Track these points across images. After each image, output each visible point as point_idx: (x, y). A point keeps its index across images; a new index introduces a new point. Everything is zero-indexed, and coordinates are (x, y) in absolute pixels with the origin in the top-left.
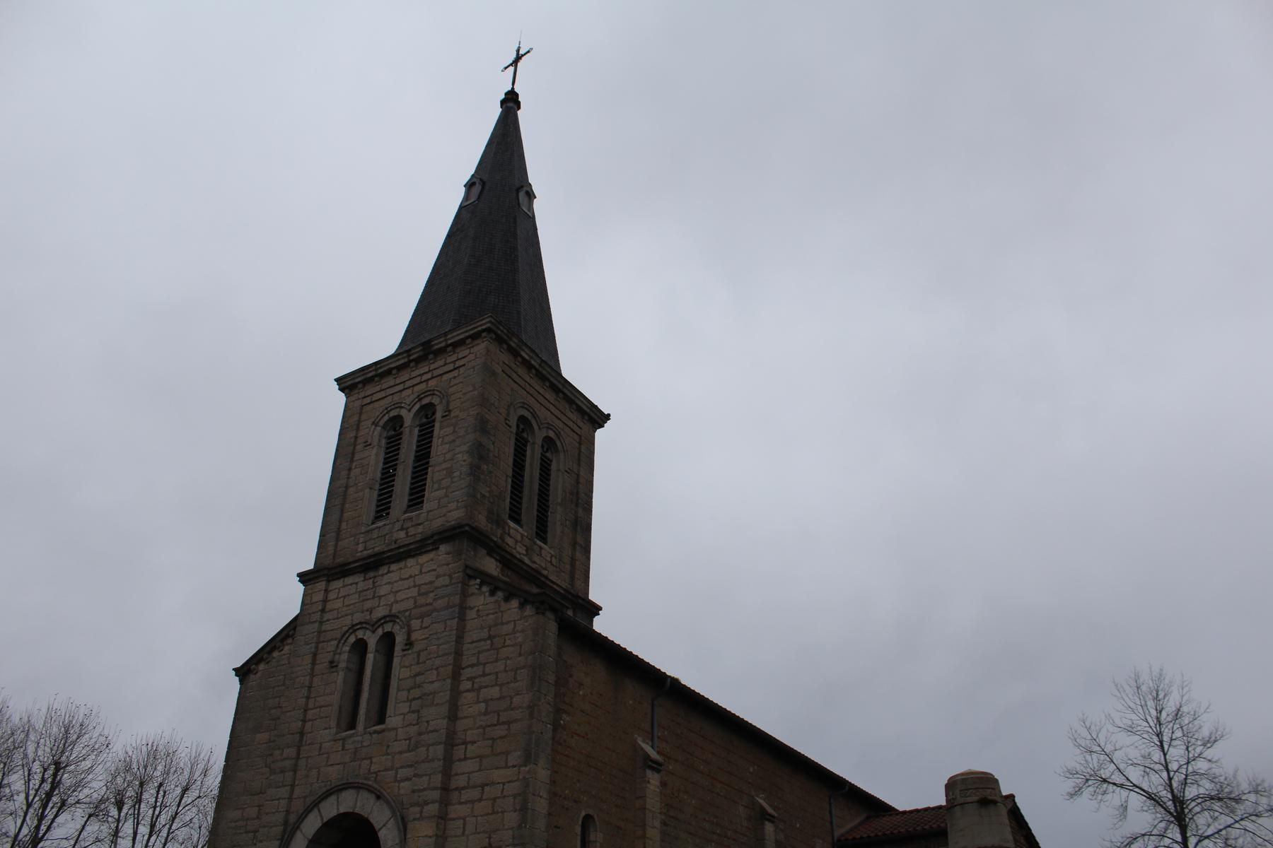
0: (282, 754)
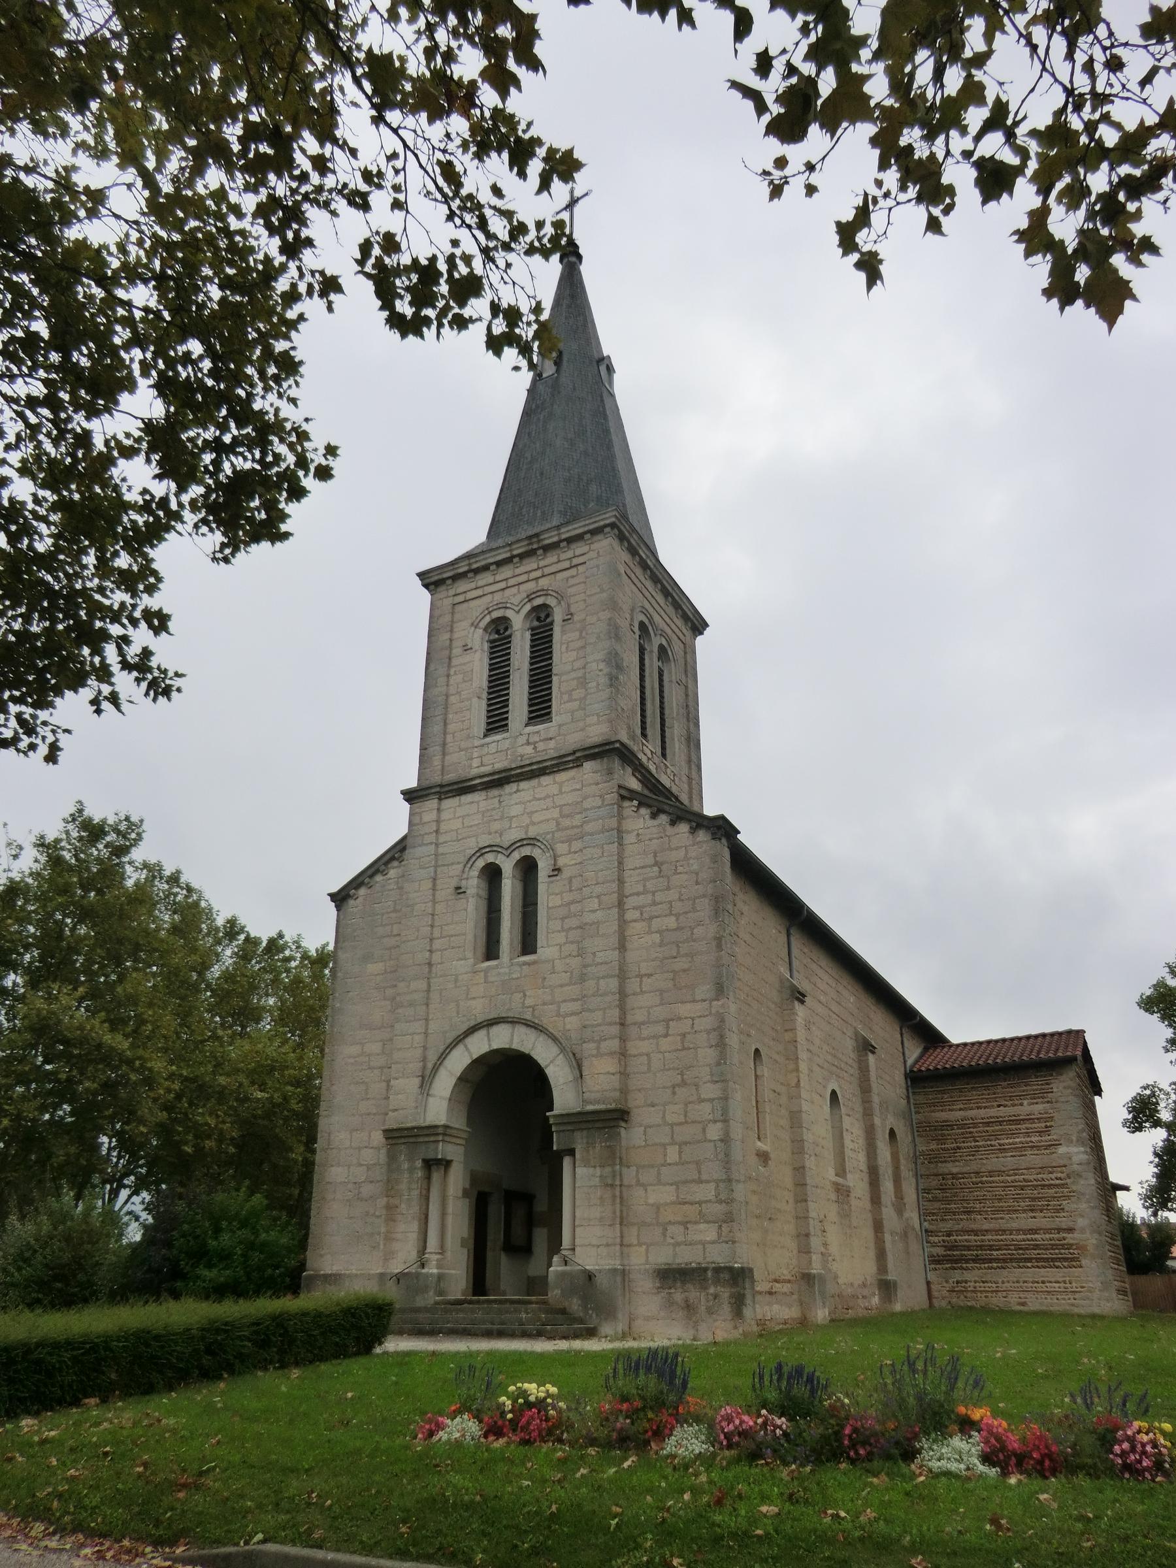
0: (408, 987)
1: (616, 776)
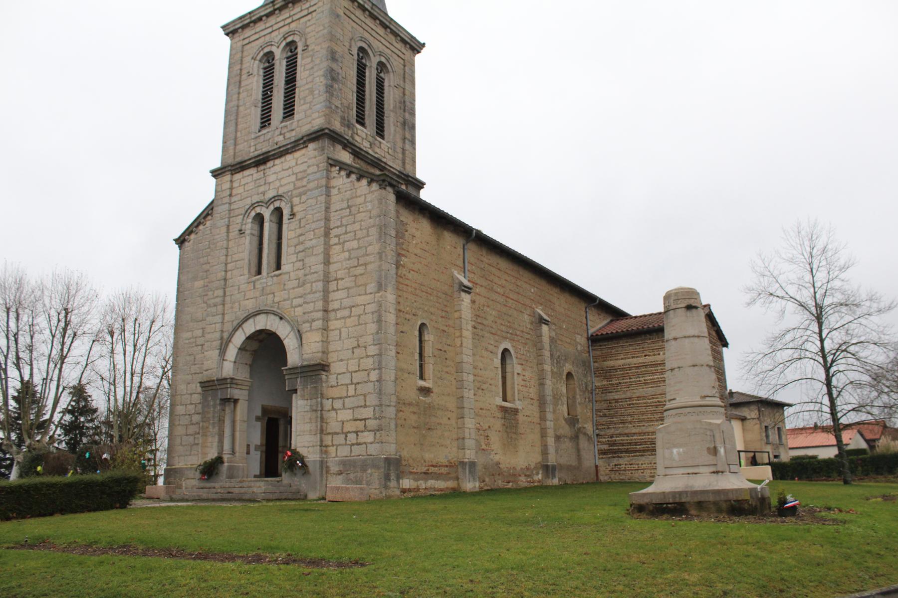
0: (213, 294)
1: (326, 151)
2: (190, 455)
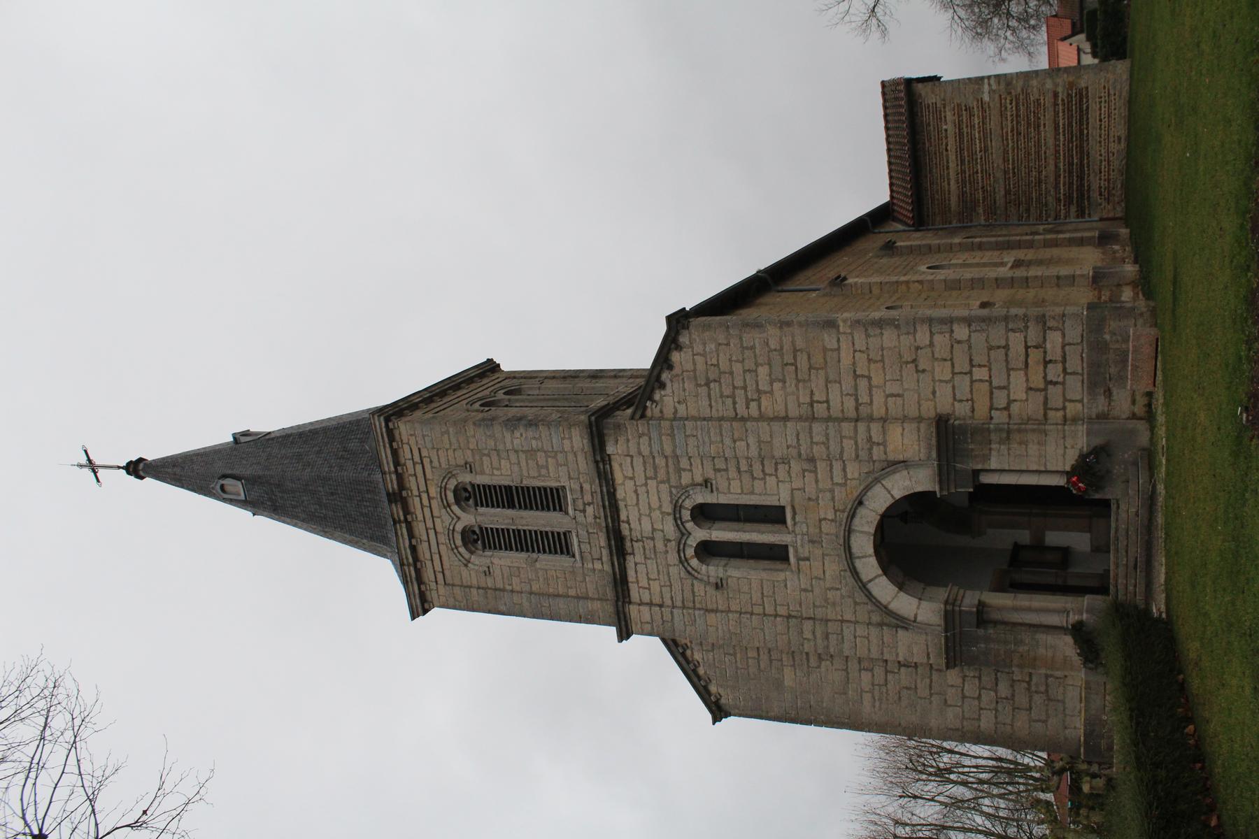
0: (809, 640)
1: (622, 422)
2: (1063, 702)
